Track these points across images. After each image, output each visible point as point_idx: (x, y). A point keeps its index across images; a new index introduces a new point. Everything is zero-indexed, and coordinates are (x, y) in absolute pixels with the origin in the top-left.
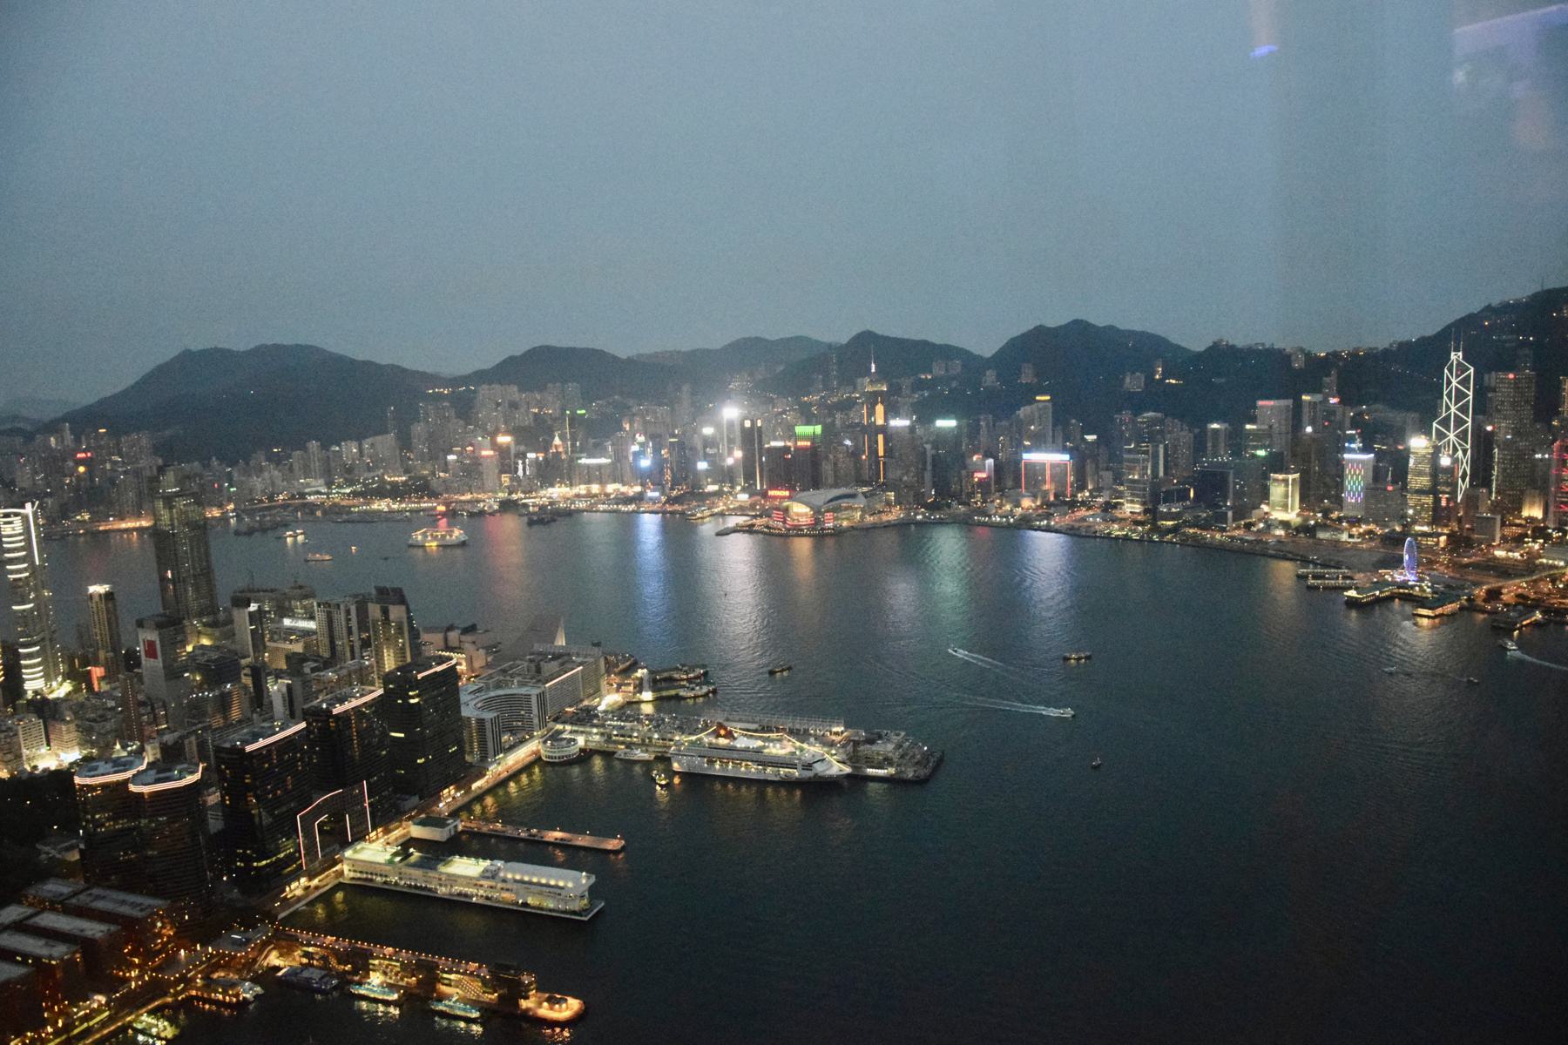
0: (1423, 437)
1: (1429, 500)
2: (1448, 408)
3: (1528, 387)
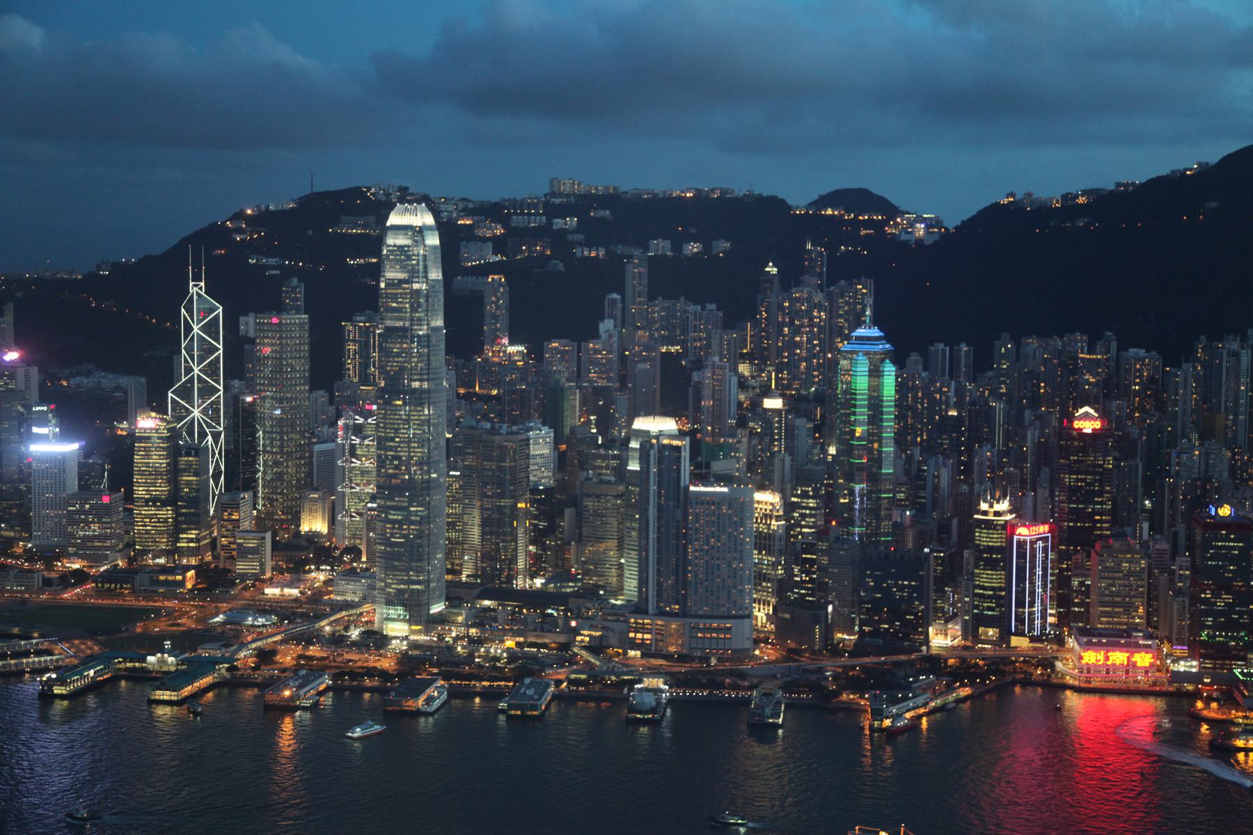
0: (153, 414)
1: (168, 513)
2: (189, 370)
3: (300, 337)
